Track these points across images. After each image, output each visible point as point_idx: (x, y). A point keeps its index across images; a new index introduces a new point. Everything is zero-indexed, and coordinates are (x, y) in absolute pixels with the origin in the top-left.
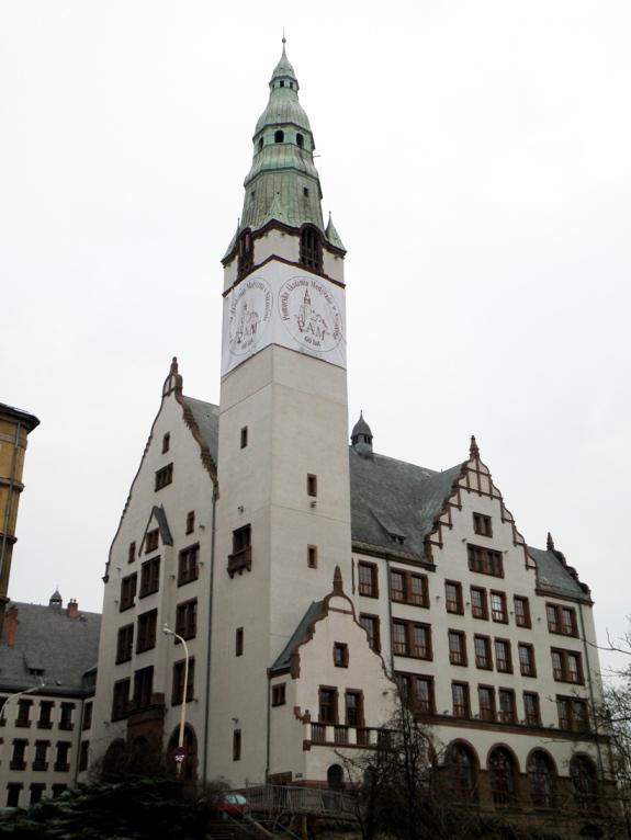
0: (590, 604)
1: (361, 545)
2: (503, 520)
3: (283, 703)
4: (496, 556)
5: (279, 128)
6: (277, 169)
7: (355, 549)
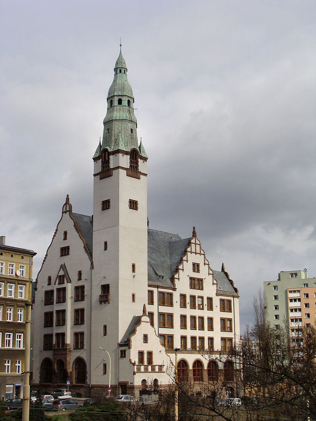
2: (205, 264)
4: (201, 281)
5: (120, 97)
6: (120, 120)
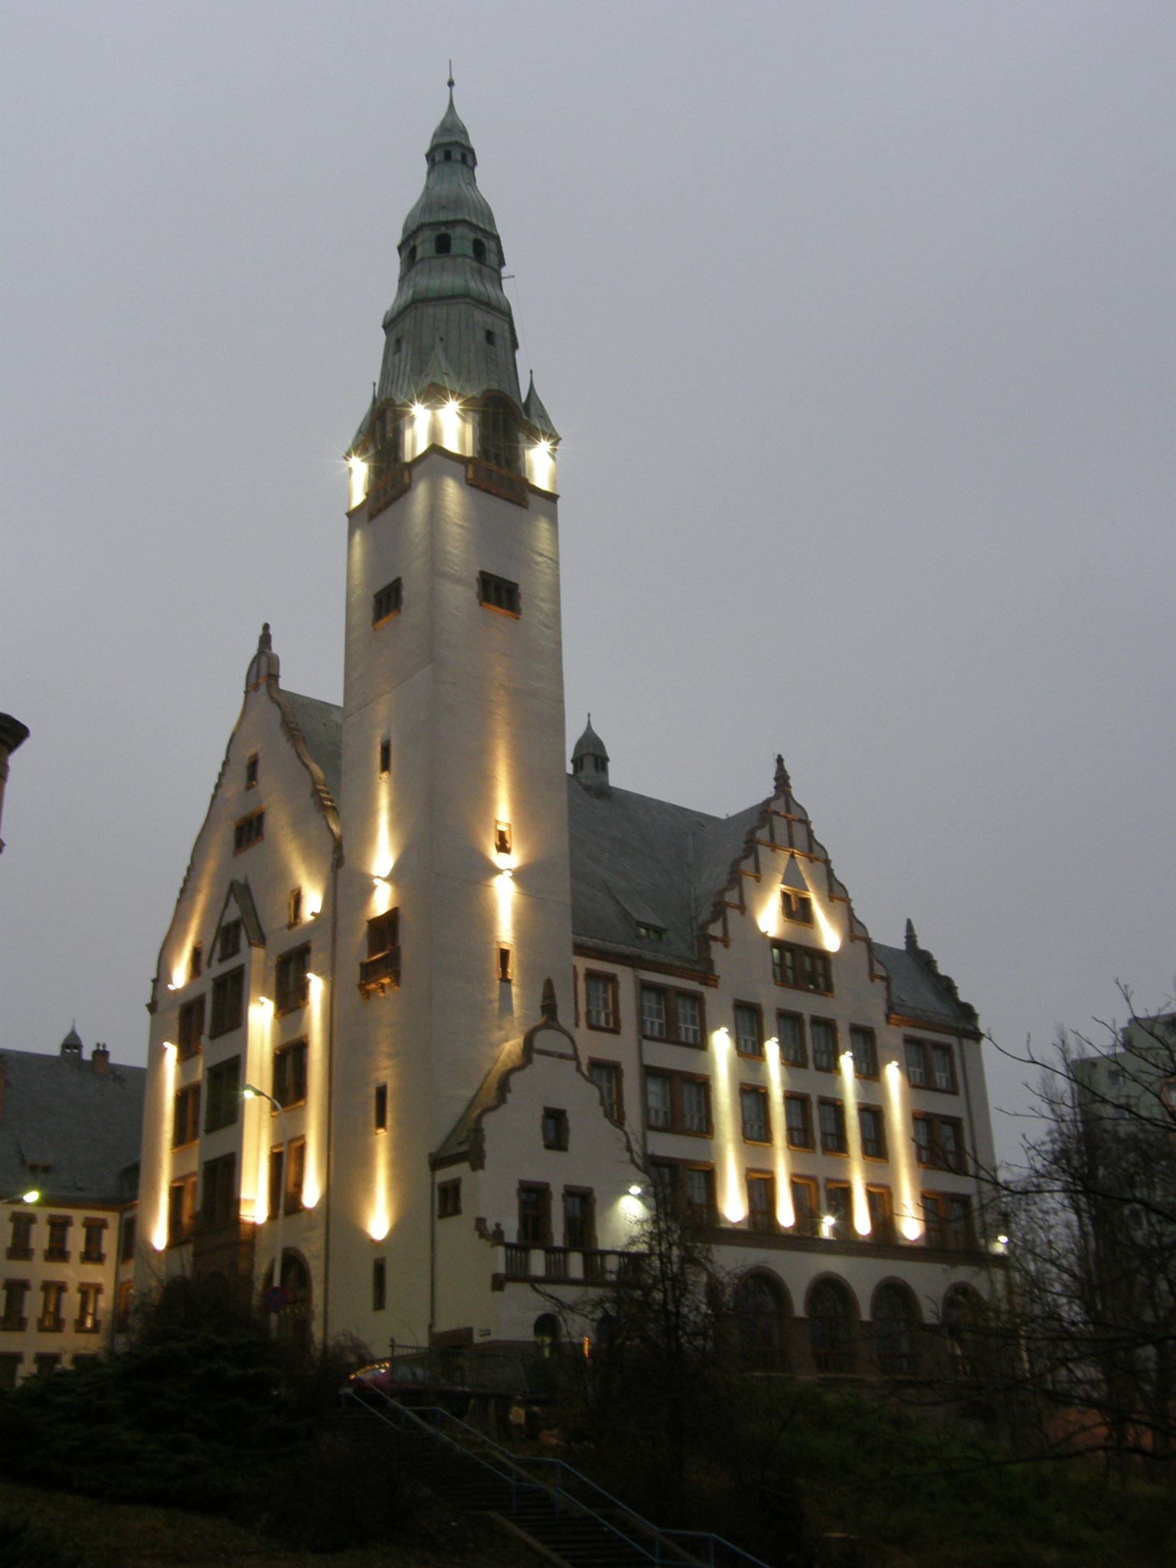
0: (977, 1036)
1: (590, 942)
3: (457, 1211)
7: (580, 950)
